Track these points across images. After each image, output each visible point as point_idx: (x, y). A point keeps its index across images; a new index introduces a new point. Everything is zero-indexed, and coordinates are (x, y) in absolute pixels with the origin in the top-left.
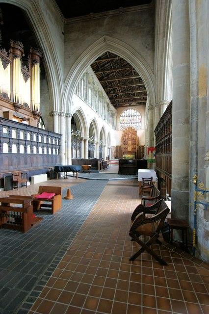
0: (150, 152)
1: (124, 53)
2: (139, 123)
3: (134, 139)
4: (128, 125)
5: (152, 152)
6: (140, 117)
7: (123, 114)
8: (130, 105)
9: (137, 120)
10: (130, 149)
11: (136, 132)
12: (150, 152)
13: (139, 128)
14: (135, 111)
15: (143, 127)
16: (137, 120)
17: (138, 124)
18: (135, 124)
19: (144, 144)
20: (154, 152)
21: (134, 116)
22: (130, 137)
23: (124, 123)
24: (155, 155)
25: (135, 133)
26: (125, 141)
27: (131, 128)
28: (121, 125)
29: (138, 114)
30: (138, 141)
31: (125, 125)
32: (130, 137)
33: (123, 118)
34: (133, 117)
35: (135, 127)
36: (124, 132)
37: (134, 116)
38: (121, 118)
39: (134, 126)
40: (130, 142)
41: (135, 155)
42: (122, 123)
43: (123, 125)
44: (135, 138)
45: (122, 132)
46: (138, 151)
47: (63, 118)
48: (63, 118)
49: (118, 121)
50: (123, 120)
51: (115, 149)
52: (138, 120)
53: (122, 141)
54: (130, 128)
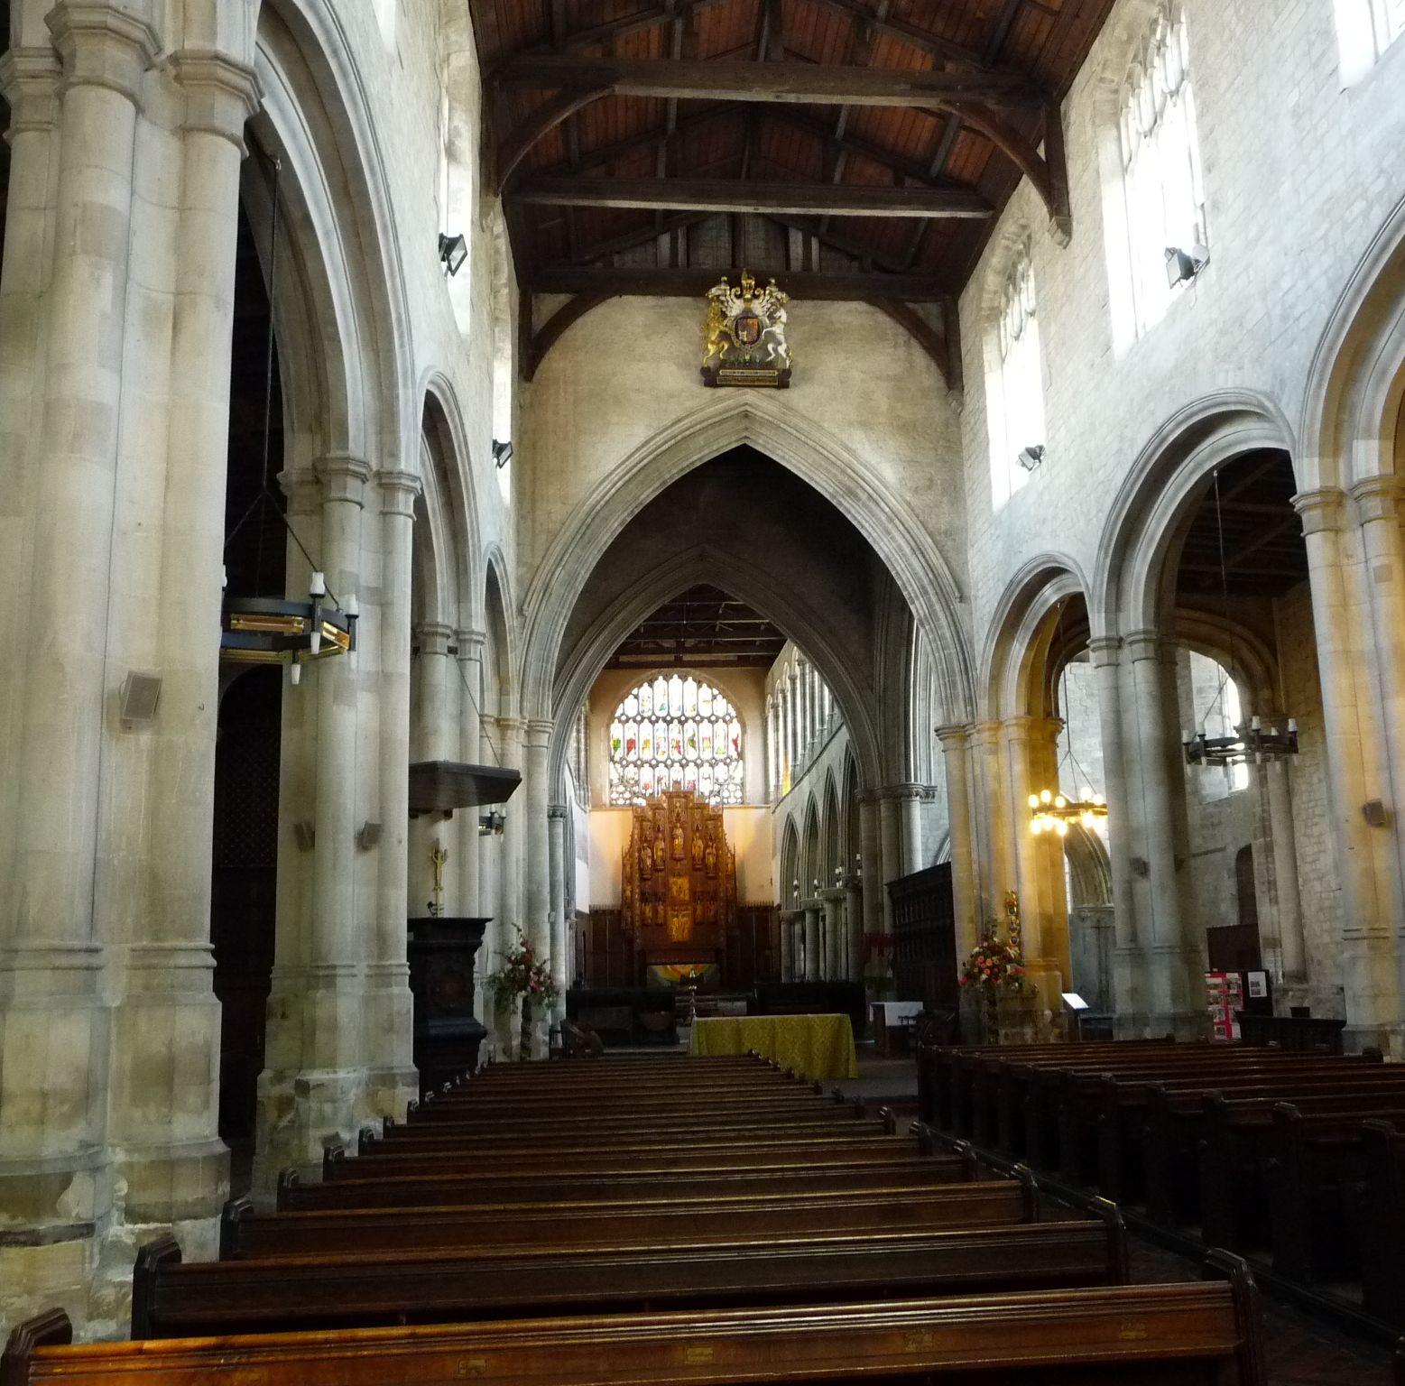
0: (875, 952)
2: (727, 762)
4: (661, 770)
5: (881, 953)
6: (735, 728)
7: (629, 706)
10: (679, 926)
11: (717, 818)
12: (875, 952)
13: (732, 794)
14: (706, 691)
17: (721, 771)
18: (706, 769)
19: (775, 896)
20: (889, 953)
21: (698, 720)
22: (679, 853)
23: (639, 764)
27: (687, 795)
28: (614, 773)
29: (722, 706)
30: (733, 876)
31: (646, 775)
33: (631, 731)
34: (690, 725)
35: (705, 787)
36: (640, 819)
37: (698, 720)
38: (616, 730)
39: (704, 784)
40: (681, 886)
43: (631, 772)
44: (711, 860)
49: (599, 750)
50: (631, 745)
52: (723, 747)
53: (627, 879)
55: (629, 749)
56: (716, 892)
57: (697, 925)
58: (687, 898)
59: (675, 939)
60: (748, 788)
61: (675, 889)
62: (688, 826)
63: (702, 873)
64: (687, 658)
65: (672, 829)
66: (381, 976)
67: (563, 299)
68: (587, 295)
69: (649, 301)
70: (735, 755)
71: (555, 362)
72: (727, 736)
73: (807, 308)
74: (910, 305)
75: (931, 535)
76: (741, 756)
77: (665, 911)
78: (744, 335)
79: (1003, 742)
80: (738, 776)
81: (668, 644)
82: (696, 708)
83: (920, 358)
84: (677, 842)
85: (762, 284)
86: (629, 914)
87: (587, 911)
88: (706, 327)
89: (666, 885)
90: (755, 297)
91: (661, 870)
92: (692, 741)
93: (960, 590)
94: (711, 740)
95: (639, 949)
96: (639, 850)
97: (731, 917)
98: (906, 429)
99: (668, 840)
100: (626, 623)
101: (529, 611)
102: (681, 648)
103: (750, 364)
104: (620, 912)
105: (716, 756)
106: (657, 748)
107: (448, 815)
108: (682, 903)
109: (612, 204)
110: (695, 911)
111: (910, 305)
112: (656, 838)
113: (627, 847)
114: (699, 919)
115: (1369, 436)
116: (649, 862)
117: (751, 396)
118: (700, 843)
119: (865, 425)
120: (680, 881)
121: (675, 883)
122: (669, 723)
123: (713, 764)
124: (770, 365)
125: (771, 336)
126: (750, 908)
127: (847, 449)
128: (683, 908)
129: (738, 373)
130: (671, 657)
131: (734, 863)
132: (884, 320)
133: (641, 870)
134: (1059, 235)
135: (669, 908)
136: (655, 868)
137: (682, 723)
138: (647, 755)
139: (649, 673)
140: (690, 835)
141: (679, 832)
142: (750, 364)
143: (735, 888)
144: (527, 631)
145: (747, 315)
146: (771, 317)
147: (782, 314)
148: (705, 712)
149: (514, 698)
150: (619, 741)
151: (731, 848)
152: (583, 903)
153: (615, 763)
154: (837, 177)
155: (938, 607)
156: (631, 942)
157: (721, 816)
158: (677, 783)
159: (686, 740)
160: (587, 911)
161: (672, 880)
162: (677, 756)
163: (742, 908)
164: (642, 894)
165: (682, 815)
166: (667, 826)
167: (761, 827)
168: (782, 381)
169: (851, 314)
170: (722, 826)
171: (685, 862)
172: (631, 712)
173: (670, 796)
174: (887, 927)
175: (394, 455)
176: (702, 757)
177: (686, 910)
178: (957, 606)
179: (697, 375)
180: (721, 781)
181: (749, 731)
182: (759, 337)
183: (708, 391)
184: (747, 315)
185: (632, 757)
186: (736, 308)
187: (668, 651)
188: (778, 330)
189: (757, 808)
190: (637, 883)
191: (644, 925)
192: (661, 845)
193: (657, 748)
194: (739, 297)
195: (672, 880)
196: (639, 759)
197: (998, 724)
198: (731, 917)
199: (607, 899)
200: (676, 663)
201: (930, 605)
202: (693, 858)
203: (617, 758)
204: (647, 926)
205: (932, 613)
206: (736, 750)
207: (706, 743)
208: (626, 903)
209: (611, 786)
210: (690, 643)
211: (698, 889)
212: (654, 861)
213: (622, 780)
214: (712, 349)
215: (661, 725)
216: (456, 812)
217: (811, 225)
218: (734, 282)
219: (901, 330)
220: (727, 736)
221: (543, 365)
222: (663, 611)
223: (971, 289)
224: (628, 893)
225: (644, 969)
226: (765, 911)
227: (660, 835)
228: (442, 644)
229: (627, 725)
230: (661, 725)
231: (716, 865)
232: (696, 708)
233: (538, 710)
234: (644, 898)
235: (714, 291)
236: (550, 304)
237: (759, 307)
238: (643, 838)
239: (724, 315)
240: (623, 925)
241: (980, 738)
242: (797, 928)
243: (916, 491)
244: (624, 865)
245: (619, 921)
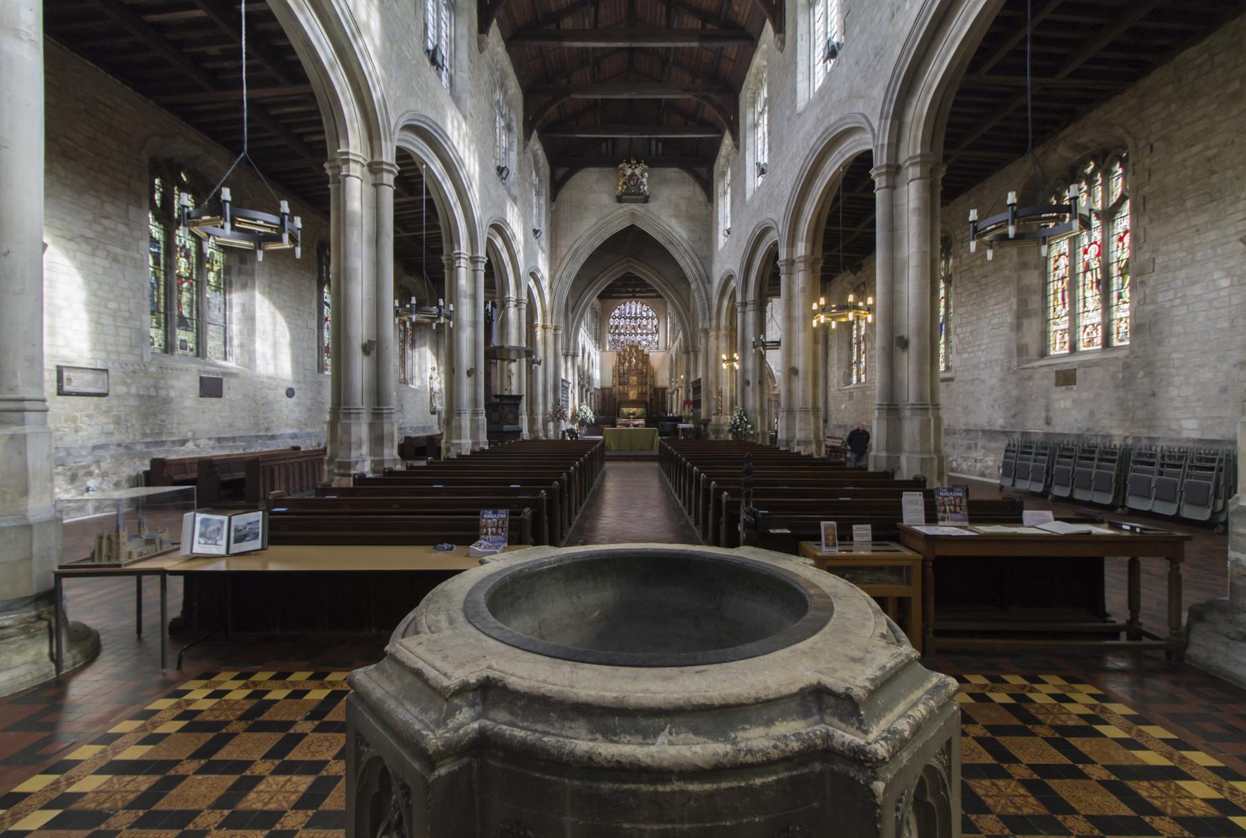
0: (687, 406)
1: (650, 279)
2: (652, 334)
3: (642, 373)
6: (655, 322)
8: (634, 297)
10: (633, 394)
11: (648, 355)
12: (687, 406)
13: (654, 345)
14: (645, 308)
15: (662, 345)
16: (650, 326)
19: (667, 384)
20: (691, 407)
21: (642, 318)
22: (633, 368)
23: (620, 334)
24: (692, 411)
25: (645, 359)
26: (621, 376)
32: (633, 368)
34: (639, 320)
36: (619, 354)
37: (642, 318)
40: (634, 379)
41: (647, 410)
42: (614, 334)
43: (616, 337)
44: (645, 370)
46: (651, 399)
47: (569, 359)
48: (569, 359)
51: (599, 393)
53: (614, 376)
54: (635, 347)
57: (640, 394)
60: (660, 344)
64: (637, 295)
66: (475, 413)
67: (567, 169)
68: (575, 168)
69: (598, 169)
71: (564, 194)
73: (656, 170)
74: (696, 169)
75: (699, 258)
76: (657, 332)
78: (632, 182)
79: (720, 335)
80: (657, 338)
81: (630, 290)
82: (641, 313)
83: (698, 190)
85: (639, 163)
87: (599, 388)
88: (619, 180)
90: (636, 167)
92: (639, 326)
93: (708, 279)
94: (648, 323)
98: (691, 218)
100: (599, 288)
101: (554, 287)
102: (634, 292)
103: (634, 194)
107: (515, 361)
108: (635, 386)
109: (578, 136)
111: (696, 169)
115: (802, 241)
117: (634, 206)
119: (676, 216)
122: (631, 319)
123: (647, 334)
124: (642, 194)
125: (642, 183)
126: (659, 389)
127: (669, 226)
129: (630, 197)
130: (631, 295)
132: (686, 175)
133: (619, 374)
134: (735, 149)
136: (624, 373)
137: (636, 318)
138: (622, 331)
139: (624, 300)
142: (631, 194)
143: (653, 381)
144: (553, 295)
145: (633, 174)
146: (642, 175)
147: (646, 174)
148: (645, 314)
149: (549, 318)
152: (597, 385)
154: (664, 122)
155: (701, 285)
158: (633, 341)
160: (599, 388)
162: (633, 331)
167: (664, 358)
168: (646, 200)
169: (672, 172)
172: (617, 315)
173: (631, 347)
174: (691, 399)
175: (477, 251)
178: (707, 286)
179: (614, 198)
182: (638, 184)
183: (619, 205)
184: (633, 174)
186: (629, 172)
187: (630, 292)
188: (644, 180)
191: (620, 393)
192: (627, 364)
194: (630, 167)
197: (718, 328)
199: (609, 384)
200: (633, 297)
201: (698, 284)
205: (698, 289)
208: (614, 385)
210: (638, 289)
213: (613, 340)
214: (620, 188)
215: (628, 320)
216: (518, 360)
217: (658, 140)
218: (628, 162)
219: (691, 179)
221: (559, 195)
222: (617, 280)
223: (717, 163)
225: (619, 410)
226: (664, 389)
228: (512, 304)
230: (628, 320)
232: (641, 313)
233: (558, 322)
234: (620, 384)
235: (621, 166)
236: (561, 172)
237: (637, 172)
238: (620, 362)
239: (625, 175)
241: (713, 334)
242: (674, 396)
243: (694, 242)
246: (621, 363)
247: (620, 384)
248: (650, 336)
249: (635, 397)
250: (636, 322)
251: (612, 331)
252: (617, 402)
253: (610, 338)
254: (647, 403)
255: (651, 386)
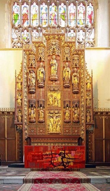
9: (81, 16)
11: (80, 53)
16: (81, 16)
17: (81, 35)
23: (30, 29)
30: (91, 91)
42: (21, 28)
43: (25, 34)
44: (75, 81)
45: (20, 53)
46: (87, 132)
53: (19, 92)
55: (24, 21)
56: (79, 102)
58: (59, 106)
59: (51, 132)
61: (51, 100)
62: (60, 58)
63: (69, 90)
65: (50, 61)
70: (90, 25)
72: (85, 13)
76: (94, 26)
77: (44, 113)
80: (92, 36)
84: (53, 68)
86: (20, 114)
89: (45, 96)
91: (42, 87)
94: (77, 13)
95: (26, 137)
96: (27, 74)
97: (89, 118)
99: (47, 68)
104: (14, 113)
105: (78, 25)
106: (41, 19)
108: (57, 108)
110: (65, 113)
112: (39, 67)
113: (18, 73)
114: (67, 119)
116: (34, 81)
118: (68, 69)
120: (55, 95)
121: (52, 96)
126: (102, 113)
128: (56, 112)
131: (91, 83)
133: (28, 86)
135: (47, 112)
138: (35, 24)
140: (62, 65)
141: (55, 62)
143: (92, 99)
150: (17, 15)
151: (90, 73)
153: (16, 29)
156: (21, 132)
157: (83, 50)
159: (60, 15)
161: (49, 94)
163: (97, 113)
164: (29, 101)
165: (56, 50)
166: (47, 59)
170: (84, 58)
171: (59, 82)
176: (69, 26)
177: (59, 113)
180: (81, 40)
181: (100, 7)
185: (26, 25)
189: (106, 49)
190: (25, 94)
193: (41, 19)
195: (49, 94)
196: (30, 27)
198: (89, 118)
202: (64, 79)
203: (16, 26)
204: (33, 122)
206: (91, 22)
207: (72, 17)
208: (20, 108)
209: (12, 42)
211: (67, 99)
212: (37, 81)
220: (85, 13)
224: (19, 101)
227: (41, 64)
229: (23, 6)
231: (79, 84)
234: (31, 106)
240: (16, 121)
244: (17, 83)
245: (14, 119)
246: (31, 69)
247: (31, 106)
248: (81, 31)
249: (58, 130)
250: (57, 10)
251: (16, 26)
252: (25, 137)
253: (15, 36)
254: (80, 139)
255: (88, 108)
